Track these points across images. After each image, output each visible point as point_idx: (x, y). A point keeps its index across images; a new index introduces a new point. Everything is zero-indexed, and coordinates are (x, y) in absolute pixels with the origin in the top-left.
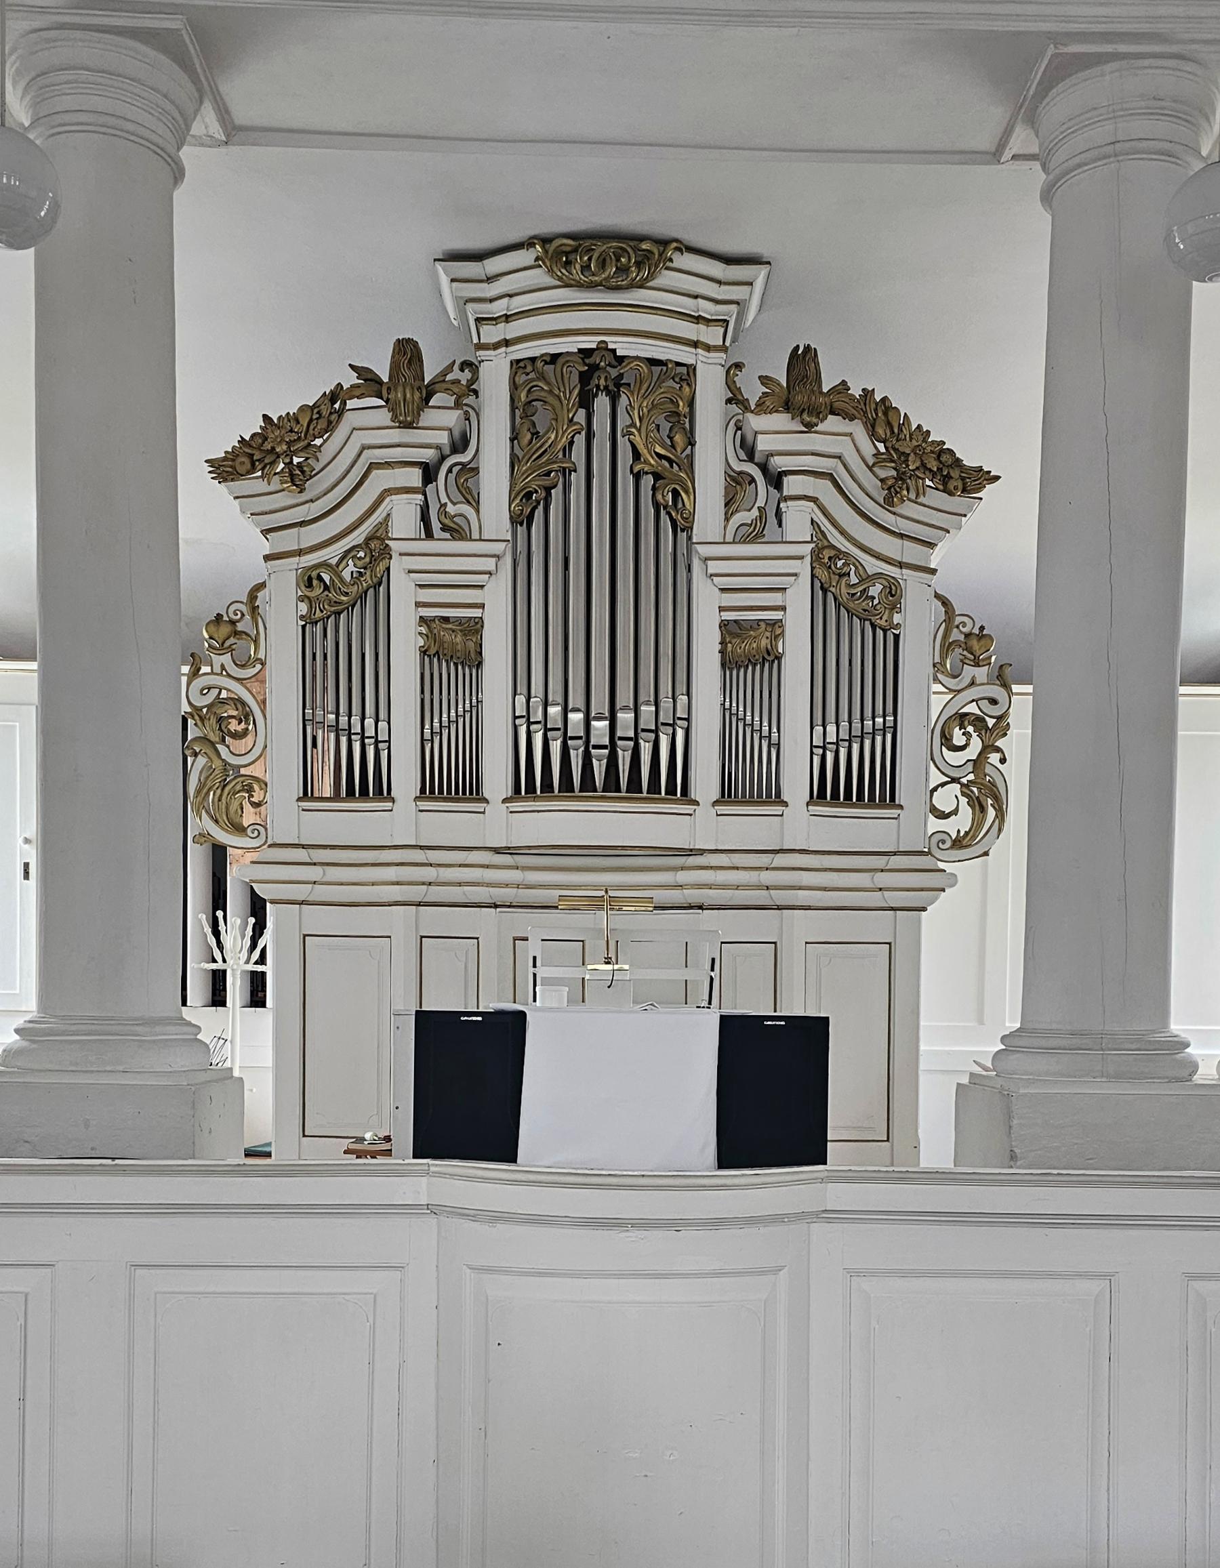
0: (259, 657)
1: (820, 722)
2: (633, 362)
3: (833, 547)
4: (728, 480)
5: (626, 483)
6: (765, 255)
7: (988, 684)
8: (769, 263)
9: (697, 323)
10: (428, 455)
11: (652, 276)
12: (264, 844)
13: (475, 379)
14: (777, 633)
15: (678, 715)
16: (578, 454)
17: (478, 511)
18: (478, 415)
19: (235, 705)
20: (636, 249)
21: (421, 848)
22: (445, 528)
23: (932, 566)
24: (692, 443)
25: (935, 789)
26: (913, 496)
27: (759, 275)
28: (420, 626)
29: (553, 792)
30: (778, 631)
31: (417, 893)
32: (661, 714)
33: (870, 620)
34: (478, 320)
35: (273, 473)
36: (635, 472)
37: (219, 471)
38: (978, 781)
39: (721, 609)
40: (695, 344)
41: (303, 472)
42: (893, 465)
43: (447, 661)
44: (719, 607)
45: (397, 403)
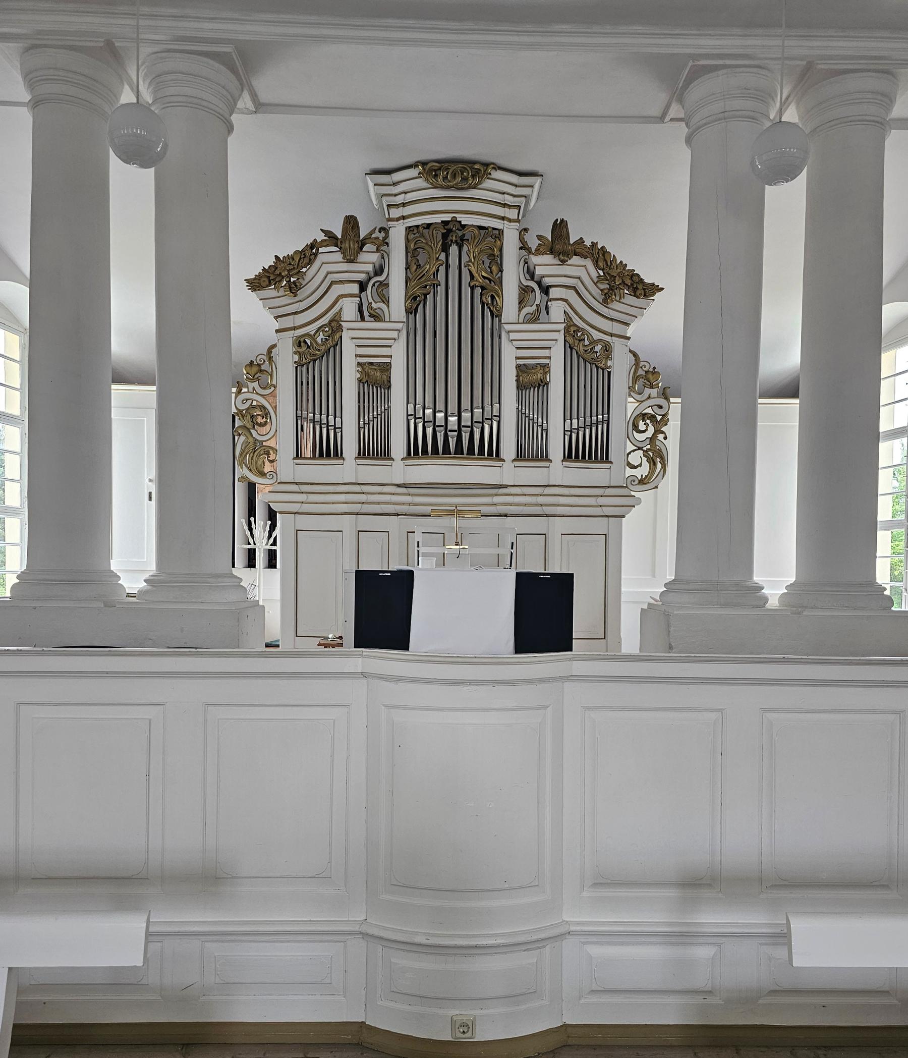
0: (273, 383)
1: (569, 418)
2: (469, 228)
3: (575, 325)
4: (520, 290)
5: (466, 291)
6: (540, 171)
7: (657, 397)
8: (542, 175)
9: (504, 207)
10: (362, 277)
11: (480, 182)
12: (276, 482)
13: (387, 237)
14: (546, 371)
15: (494, 414)
16: (441, 276)
17: (388, 306)
18: (388, 256)
19: (260, 409)
20: (472, 168)
21: (358, 484)
22: (371, 316)
23: (628, 335)
24: (501, 271)
25: (630, 453)
26: (618, 298)
27: (537, 181)
29: (428, 455)
30: (547, 370)
31: (356, 508)
32: (485, 413)
33: (595, 364)
34: (388, 206)
35: (280, 286)
36: (471, 285)
37: (251, 285)
38: (652, 449)
39: (517, 358)
40: (503, 218)
41: (296, 286)
42: (607, 282)
43: (372, 386)
44: (516, 357)
45: (346, 249)
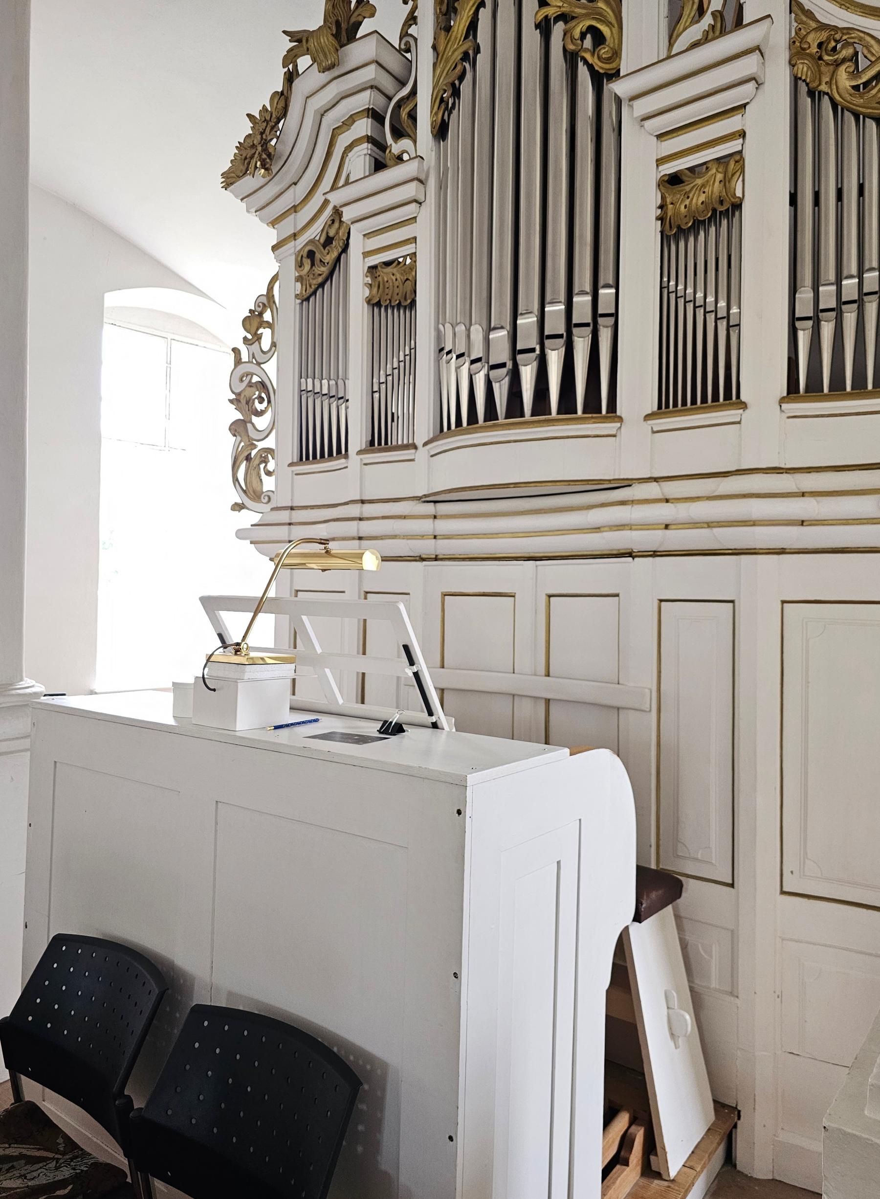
10: (364, 100)
28: (367, 277)
39: (660, 161)
